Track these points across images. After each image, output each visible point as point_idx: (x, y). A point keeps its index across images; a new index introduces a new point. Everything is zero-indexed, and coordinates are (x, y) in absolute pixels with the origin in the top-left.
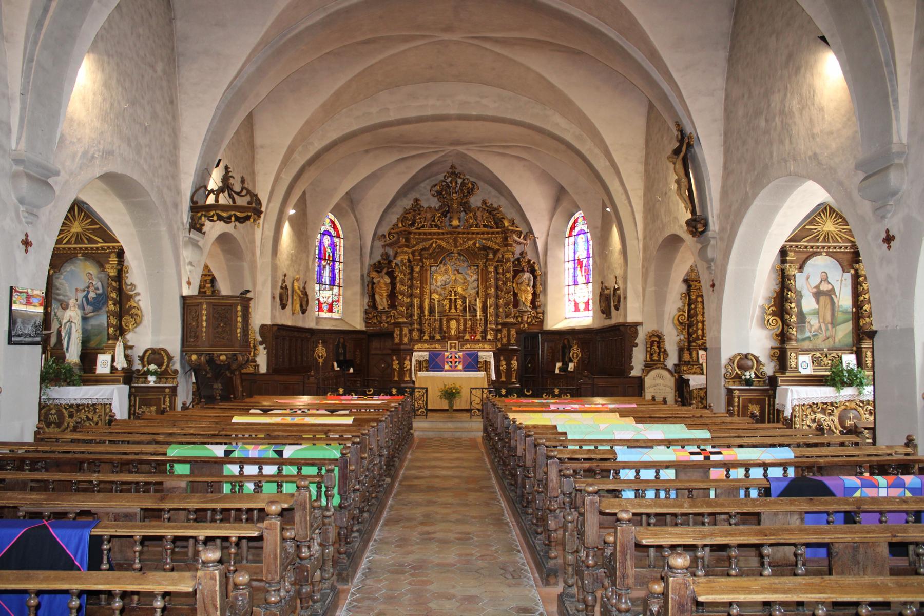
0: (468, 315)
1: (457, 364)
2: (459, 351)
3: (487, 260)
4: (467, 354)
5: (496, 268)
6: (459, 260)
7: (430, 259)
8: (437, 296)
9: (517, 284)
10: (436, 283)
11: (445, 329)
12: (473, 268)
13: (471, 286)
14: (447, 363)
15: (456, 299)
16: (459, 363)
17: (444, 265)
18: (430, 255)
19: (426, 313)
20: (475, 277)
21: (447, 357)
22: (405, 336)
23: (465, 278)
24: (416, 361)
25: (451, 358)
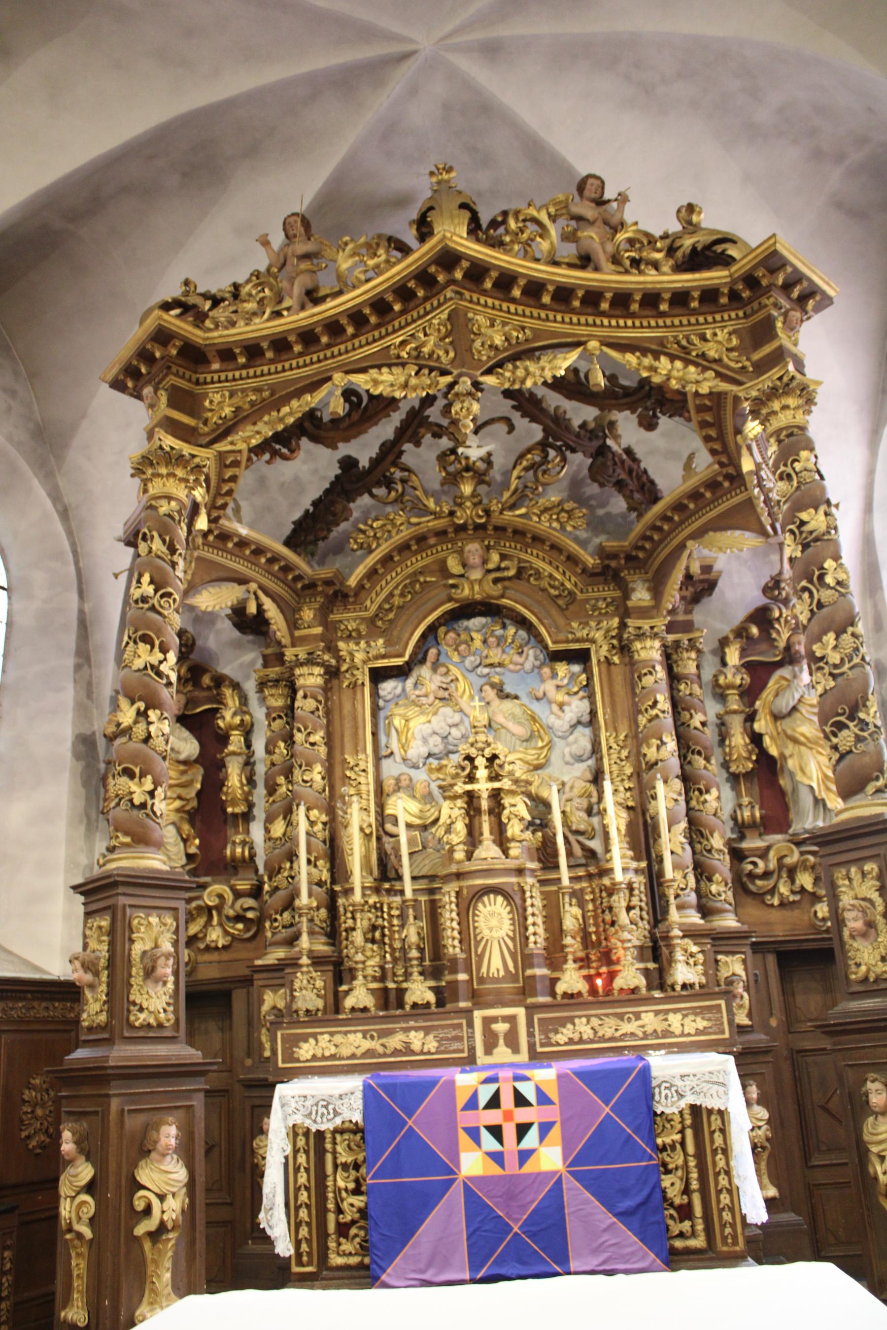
0: (565, 874)
1: (531, 1139)
2: (537, 1058)
3: (625, 613)
4: (582, 1075)
5: (669, 656)
6: (500, 640)
7: (371, 636)
8: (414, 806)
9: (777, 717)
10: (404, 747)
11: (453, 947)
12: (562, 669)
13: (563, 750)
14: (474, 1134)
15: (496, 795)
16: (545, 1129)
17: (435, 667)
18: (371, 621)
19: (358, 878)
20: (578, 707)
21: (472, 1103)
22: (149, 973)
23: (534, 719)
24: (294, 1132)
25: (494, 1102)
